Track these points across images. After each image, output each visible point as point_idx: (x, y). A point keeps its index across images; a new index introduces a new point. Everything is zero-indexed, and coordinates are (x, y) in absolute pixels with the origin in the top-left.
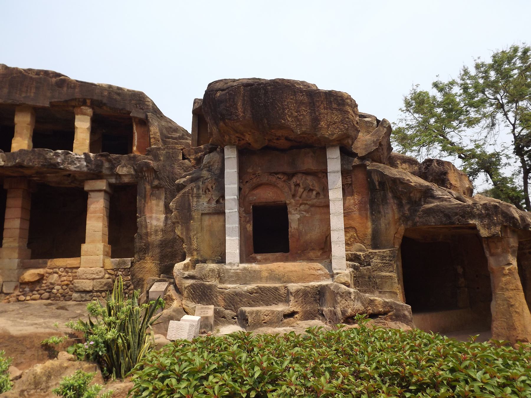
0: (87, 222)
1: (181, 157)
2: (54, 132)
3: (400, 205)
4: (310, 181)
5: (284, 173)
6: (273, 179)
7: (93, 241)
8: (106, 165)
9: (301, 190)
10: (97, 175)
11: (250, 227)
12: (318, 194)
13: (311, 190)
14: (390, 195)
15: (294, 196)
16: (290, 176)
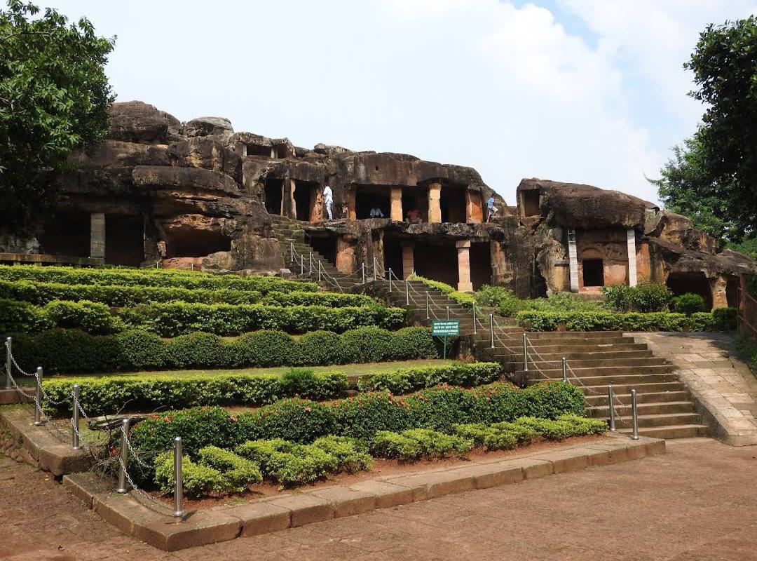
1: (519, 225)
2: (415, 202)
4: (617, 246)
5: (601, 242)
6: (595, 246)
10: (465, 238)
12: (621, 254)
13: (617, 252)
15: (607, 255)
16: (605, 244)
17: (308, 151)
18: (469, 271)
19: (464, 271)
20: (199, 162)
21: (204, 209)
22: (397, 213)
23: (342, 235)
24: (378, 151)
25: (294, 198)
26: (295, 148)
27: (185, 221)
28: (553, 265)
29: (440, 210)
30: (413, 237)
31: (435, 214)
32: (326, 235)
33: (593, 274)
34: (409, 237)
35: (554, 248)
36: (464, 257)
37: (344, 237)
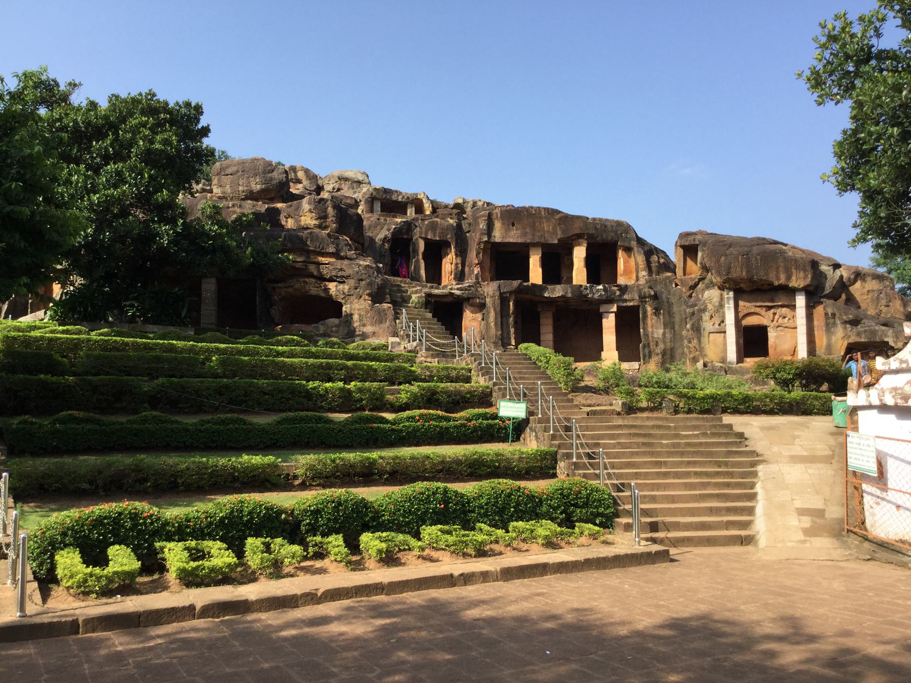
0: (604, 336)
3: (845, 328)
6: (758, 310)
7: (609, 350)
8: (618, 293)
9: (777, 317)
10: (609, 301)
11: (741, 341)
13: (785, 317)
14: (838, 322)
15: (773, 321)
17: (446, 207)
18: (614, 338)
19: (609, 338)
20: (315, 222)
21: (315, 273)
22: (536, 275)
23: (468, 299)
24: (517, 205)
25: (423, 258)
26: (432, 202)
27: (297, 286)
28: (706, 334)
29: (585, 269)
30: (551, 301)
31: (579, 275)
32: (451, 299)
33: (753, 341)
34: (544, 300)
35: (707, 313)
36: (609, 323)
37: (471, 301)
